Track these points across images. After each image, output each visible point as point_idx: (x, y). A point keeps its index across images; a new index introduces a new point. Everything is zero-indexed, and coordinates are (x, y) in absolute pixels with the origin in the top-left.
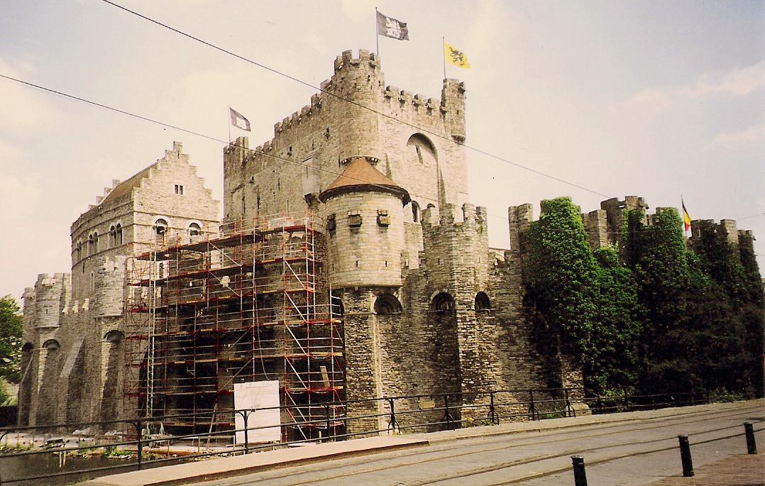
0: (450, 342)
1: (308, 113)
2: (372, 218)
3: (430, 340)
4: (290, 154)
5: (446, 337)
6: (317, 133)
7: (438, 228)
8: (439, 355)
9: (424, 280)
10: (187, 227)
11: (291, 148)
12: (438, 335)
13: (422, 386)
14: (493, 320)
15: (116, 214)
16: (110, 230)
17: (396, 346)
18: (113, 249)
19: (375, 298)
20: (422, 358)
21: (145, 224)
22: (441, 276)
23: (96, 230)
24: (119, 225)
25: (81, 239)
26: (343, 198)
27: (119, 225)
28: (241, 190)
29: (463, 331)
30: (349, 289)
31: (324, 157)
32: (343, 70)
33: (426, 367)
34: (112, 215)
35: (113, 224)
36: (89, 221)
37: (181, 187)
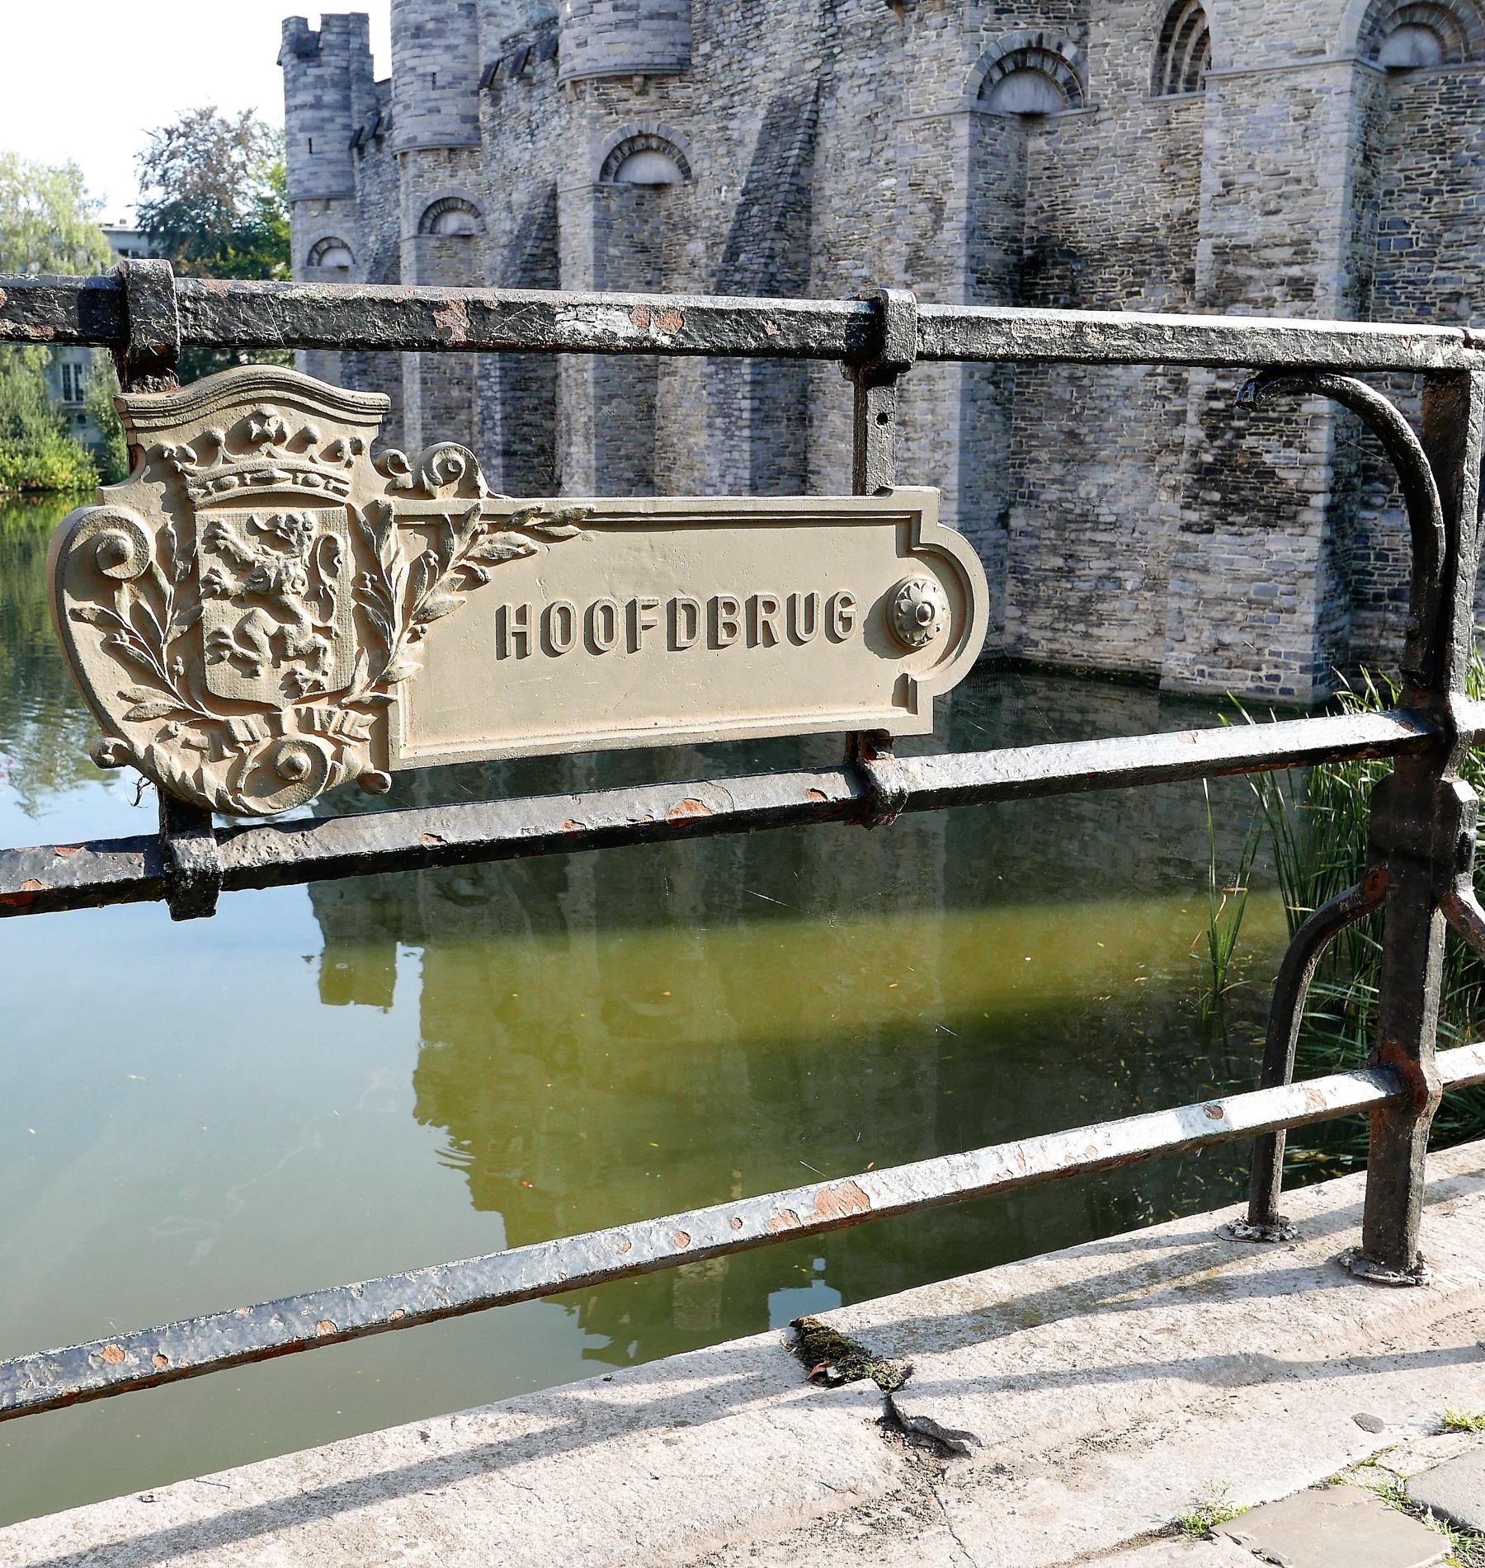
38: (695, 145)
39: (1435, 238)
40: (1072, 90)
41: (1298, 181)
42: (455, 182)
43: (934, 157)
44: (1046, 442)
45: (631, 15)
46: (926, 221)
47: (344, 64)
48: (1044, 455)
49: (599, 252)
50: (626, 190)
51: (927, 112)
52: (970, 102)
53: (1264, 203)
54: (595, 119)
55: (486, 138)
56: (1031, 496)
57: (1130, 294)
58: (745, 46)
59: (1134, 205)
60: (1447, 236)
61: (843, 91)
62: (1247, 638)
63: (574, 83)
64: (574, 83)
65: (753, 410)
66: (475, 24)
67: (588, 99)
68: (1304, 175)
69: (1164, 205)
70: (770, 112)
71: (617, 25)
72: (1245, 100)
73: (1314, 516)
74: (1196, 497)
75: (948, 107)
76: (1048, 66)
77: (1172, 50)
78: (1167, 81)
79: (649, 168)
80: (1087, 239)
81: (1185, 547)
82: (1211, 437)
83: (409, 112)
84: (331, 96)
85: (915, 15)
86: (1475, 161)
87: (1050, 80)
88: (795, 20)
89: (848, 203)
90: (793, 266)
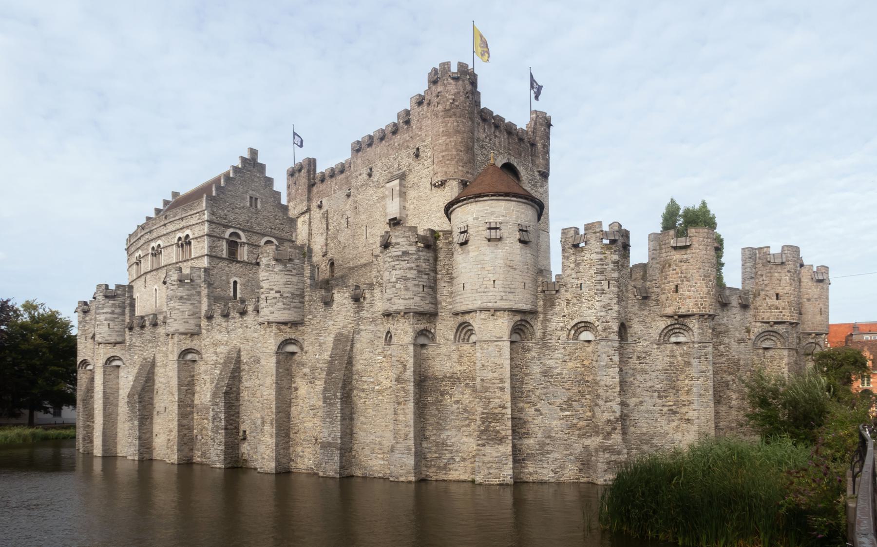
4: (370, 175)
10: (262, 243)
11: (371, 169)
16: (176, 242)
18: (186, 261)
21: (218, 235)
23: (159, 242)
24: (187, 236)
25: (140, 252)
27: (187, 236)
31: (411, 179)
36: (150, 232)
37: (256, 199)
38: (306, 342)
39: (523, 379)
40: (433, 339)
41: (499, 365)
42: (192, 344)
43: (404, 354)
44: (431, 425)
45: (289, 307)
46: (401, 369)
47: (123, 301)
48: (430, 428)
49: (277, 371)
50: (284, 353)
51: (401, 343)
52: (412, 342)
53: (492, 370)
54: (276, 334)
55: (204, 332)
56: (427, 438)
57: (451, 389)
58: (326, 318)
59: (451, 368)
60: (526, 378)
61: (363, 333)
62: (496, 471)
63: (268, 323)
64: (268, 323)
65: (341, 417)
66: (200, 298)
67: (274, 328)
68: (500, 363)
69: (458, 368)
70: (336, 336)
71: (284, 309)
72: (485, 347)
73: (509, 441)
74: (480, 438)
75: (407, 342)
76: (428, 334)
78: (457, 339)
79: (291, 348)
80: (439, 375)
81: (479, 450)
82: (483, 423)
83: (176, 322)
84: (118, 310)
85: (396, 319)
86: (530, 362)
87: (428, 337)
88: (345, 314)
89: (366, 362)
90: (349, 378)
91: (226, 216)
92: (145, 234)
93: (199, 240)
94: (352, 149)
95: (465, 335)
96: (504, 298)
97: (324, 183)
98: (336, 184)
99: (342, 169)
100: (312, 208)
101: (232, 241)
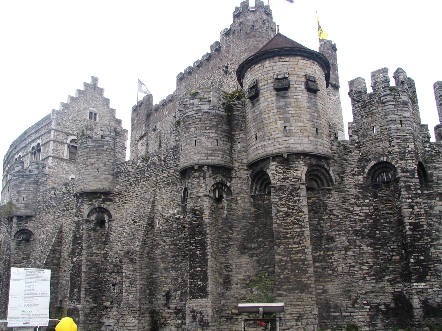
0: (388, 218)
1: (208, 58)
2: (300, 83)
3: (367, 215)
5: (384, 212)
6: (216, 73)
7: (371, 95)
8: (377, 232)
9: (357, 152)
12: (375, 210)
13: (360, 268)
14: (431, 194)
15: (37, 135)
16: (31, 150)
17: (328, 224)
19: (306, 169)
20: (358, 236)
21: (61, 141)
22: (377, 144)
24: (39, 144)
26: (267, 64)
27: (39, 144)
28: (145, 139)
29: (409, 201)
30: (276, 157)
32: (241, 16)
33: (364, 247)
34: (32, 138)
35: (34, 144)
36: (15, 148)
37: (95, 114)
77: (255, 184)
91: (68, 126)
92: (12, 150)
93: (46, 145)
94: (177, 79)
95: (261, 186)
96: (297, 142)
97: (158, 112)
98: (167, 111)
99: (171, 99)
100: (149, 132)
101: (72, 146)
